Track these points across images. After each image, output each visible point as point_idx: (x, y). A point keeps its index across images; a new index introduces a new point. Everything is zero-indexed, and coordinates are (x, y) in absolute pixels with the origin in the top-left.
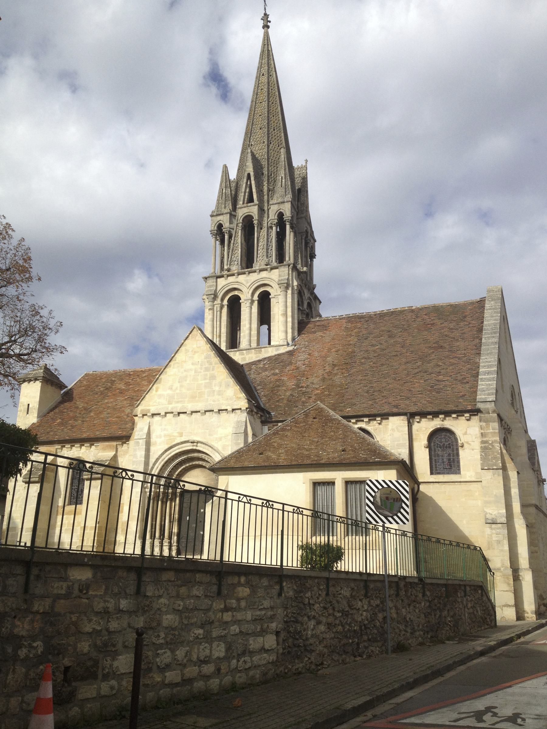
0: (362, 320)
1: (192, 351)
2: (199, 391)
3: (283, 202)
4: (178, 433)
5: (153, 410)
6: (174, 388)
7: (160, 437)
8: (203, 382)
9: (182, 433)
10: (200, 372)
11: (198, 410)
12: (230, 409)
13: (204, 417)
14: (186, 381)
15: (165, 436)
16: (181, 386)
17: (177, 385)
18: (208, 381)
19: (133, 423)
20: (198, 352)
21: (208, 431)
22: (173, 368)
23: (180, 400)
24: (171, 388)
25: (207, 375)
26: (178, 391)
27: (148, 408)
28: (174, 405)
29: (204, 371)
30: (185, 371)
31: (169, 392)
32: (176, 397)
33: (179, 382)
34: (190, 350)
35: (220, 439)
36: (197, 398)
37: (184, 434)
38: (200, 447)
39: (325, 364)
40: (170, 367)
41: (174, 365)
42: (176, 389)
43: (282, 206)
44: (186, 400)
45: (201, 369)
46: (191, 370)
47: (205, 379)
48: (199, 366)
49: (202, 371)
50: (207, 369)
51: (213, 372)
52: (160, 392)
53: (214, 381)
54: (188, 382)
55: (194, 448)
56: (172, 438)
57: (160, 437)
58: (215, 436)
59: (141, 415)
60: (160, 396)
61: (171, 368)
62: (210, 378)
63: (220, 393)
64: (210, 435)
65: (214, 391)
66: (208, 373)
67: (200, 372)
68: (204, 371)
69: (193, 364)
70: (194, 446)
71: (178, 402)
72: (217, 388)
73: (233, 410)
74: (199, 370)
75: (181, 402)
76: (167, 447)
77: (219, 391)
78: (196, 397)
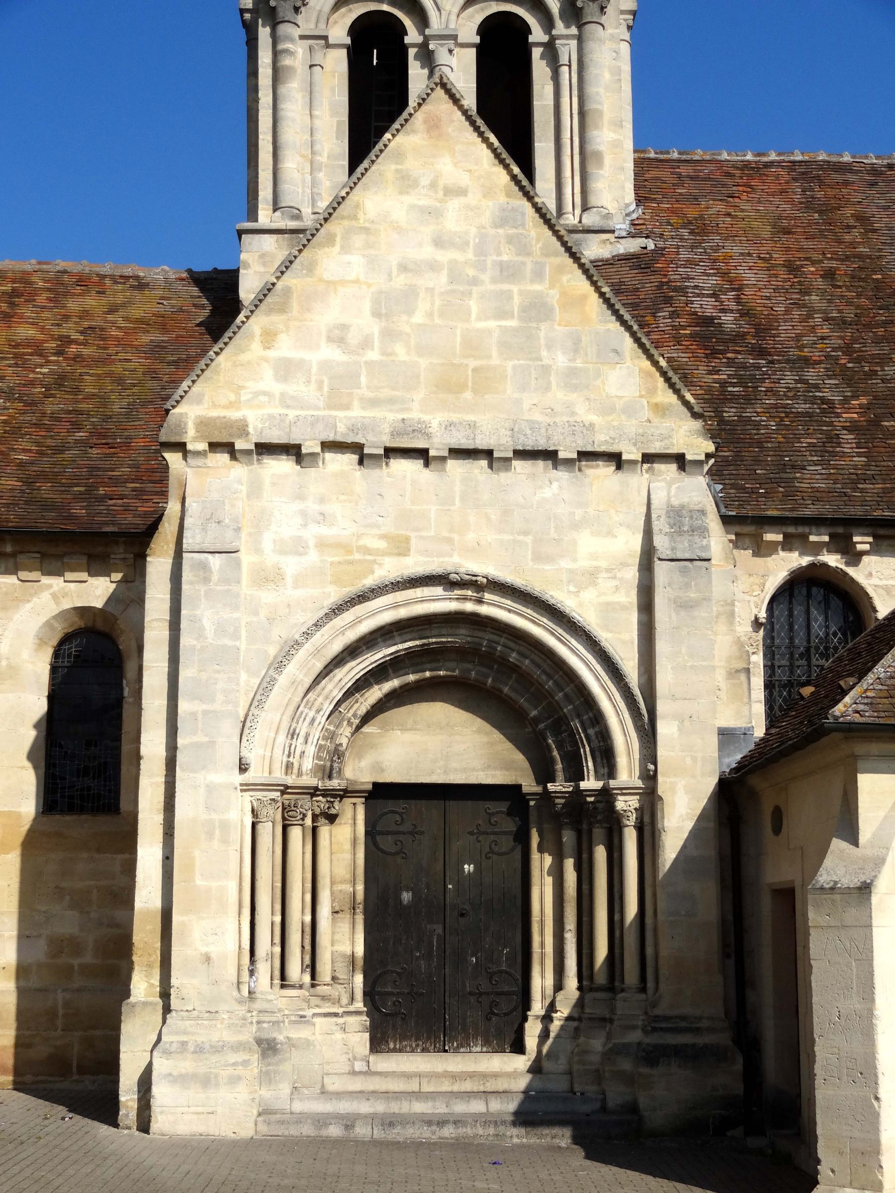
0: (850, 177)
1: (433, 185)
2: (473, 363)
4: (383, 537)
5: (260, 424)
6: (353, 338)
7: (298, 547)
8: (492, 324)
9: (407, 540)
10: (475, 282)
11: (481, 443)
13: (504, 477)
14: (410, 312)
15: (322, 545)
16: (389, 335)
17: (365, 323)
18: (513, 323)
19: (159, 477)
20: (461, 192)
21: (529, 539)
22: (345, 250)
23: (386, 393)
24: (338, 336)
25: (509, 296)
26: (373, 355)
27: (234, 415)
28: (357, 413)
29: (494, 281)
30: (404, 268)
31: (333, 354)
32: (363, 380)
33: (377, 314)
34: (425, 181)
35: (592, 575)
36: (468, 395)
37: (413, 542)
38: (495, 608)
39: (809, 316)
40: (331, 240)
41: (347, 233)
42: (366, 343)
44: (418, 396)
45: (481, 266)
46: (433, 266)
47: (502, 314)
48: (470, 255)
49: (485, 277)
50: (508, 272)
51: (537, 287)
52: (285, 347)
53: (544, 326)
54: (418, 318)
55: (469, 607)
56: (357, 556)
57: (298, 547)
58: (565, 564)
59: (203, 446)
60: (286, 369)
61: (337, 248)
62: (524, 309)
63: (573, 379)
64: (538, 557)
65: (546, 370)
66: (515, 289)
67: (475, 282)
68: (494, 281)
69: (439, 242)
70: (465, 599)
71: (374, 403)
72: (561, 360)
73: (648, 458)
74: (471, 272)
75: (392, 401)
76: (335, 594)
77: (572, 372)
78: (461, 388)
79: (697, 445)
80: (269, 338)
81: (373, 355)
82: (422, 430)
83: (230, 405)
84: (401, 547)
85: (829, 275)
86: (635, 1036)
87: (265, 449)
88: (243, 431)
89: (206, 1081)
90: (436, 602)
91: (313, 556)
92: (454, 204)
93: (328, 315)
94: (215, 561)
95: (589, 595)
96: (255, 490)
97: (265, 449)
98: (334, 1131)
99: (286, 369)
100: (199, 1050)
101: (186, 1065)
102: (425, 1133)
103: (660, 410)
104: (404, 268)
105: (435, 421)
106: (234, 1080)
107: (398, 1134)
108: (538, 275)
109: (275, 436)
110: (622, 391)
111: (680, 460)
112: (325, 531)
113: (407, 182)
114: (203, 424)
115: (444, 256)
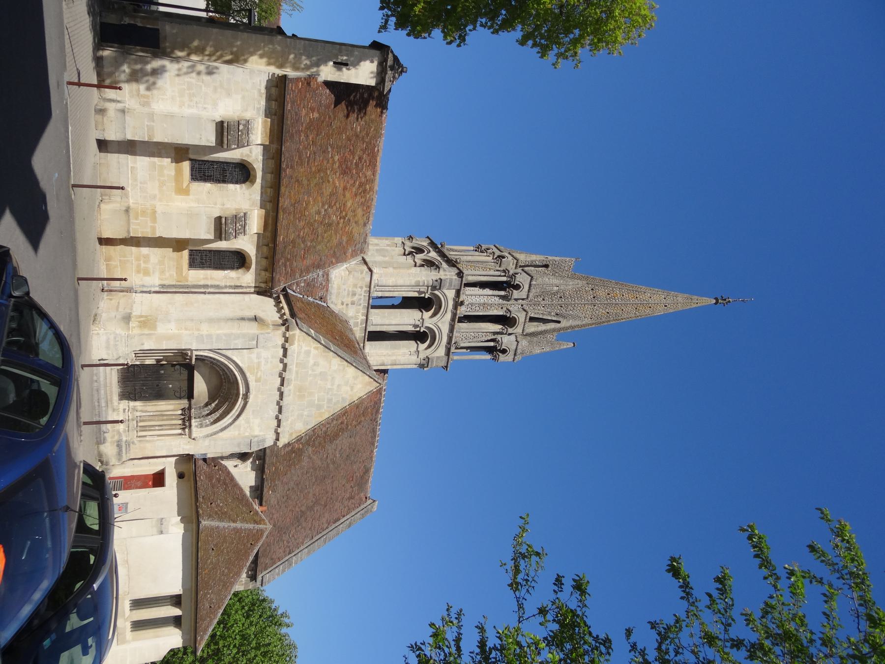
3: (515, 355)
5: (293, 349)
12: (279, 430)
15: (259, 364)
17: (319, 370)
22: (339, 365)
24: (316, 364)
26: (310, 372)
31: (312, 362)
38: (240, 402)
42: (313, 370)
43: (512, 353)
46: (333, 385)
47: (318, 400)
50: (330, 401)
52: (314, 352)
54: (319, 382)
57: (258, 357)
60: (308, 353)
64: (253, 411)
69: (339, 386)
71: (297, 373)
72: (306, 413)
79: (280, 444)
80: (316, 348)
81: (310, 372)
82: (289, 385)
83: (299, 340)
84: (258, 380)
85: (342, 423)
86: (124, 439)
87: (285, 350)
88: (291, 345)
89: (108, 348)
90: (242, 390)
91: (256, 361)
92: (349, 389)
93: (322, 362)
94: (255, 342)
95: (243, 422)
96: (275, 347)
97: (285, 350)
98: (95, 378)
99: (308, 353)
100: (116, 345)
101: (112, 343)
102: (96, 398)
103: (291, 434)
104: (333, 378)
105: (291, 387)
106: (108, 354)
107: (95, 393)
108: (328, 407)
109: (289, 353)
110: (296, 425)
111: (277, 439)
112: (263, 364)
113: (355, 378)
114: (294, 335)
115: (335, 387)
